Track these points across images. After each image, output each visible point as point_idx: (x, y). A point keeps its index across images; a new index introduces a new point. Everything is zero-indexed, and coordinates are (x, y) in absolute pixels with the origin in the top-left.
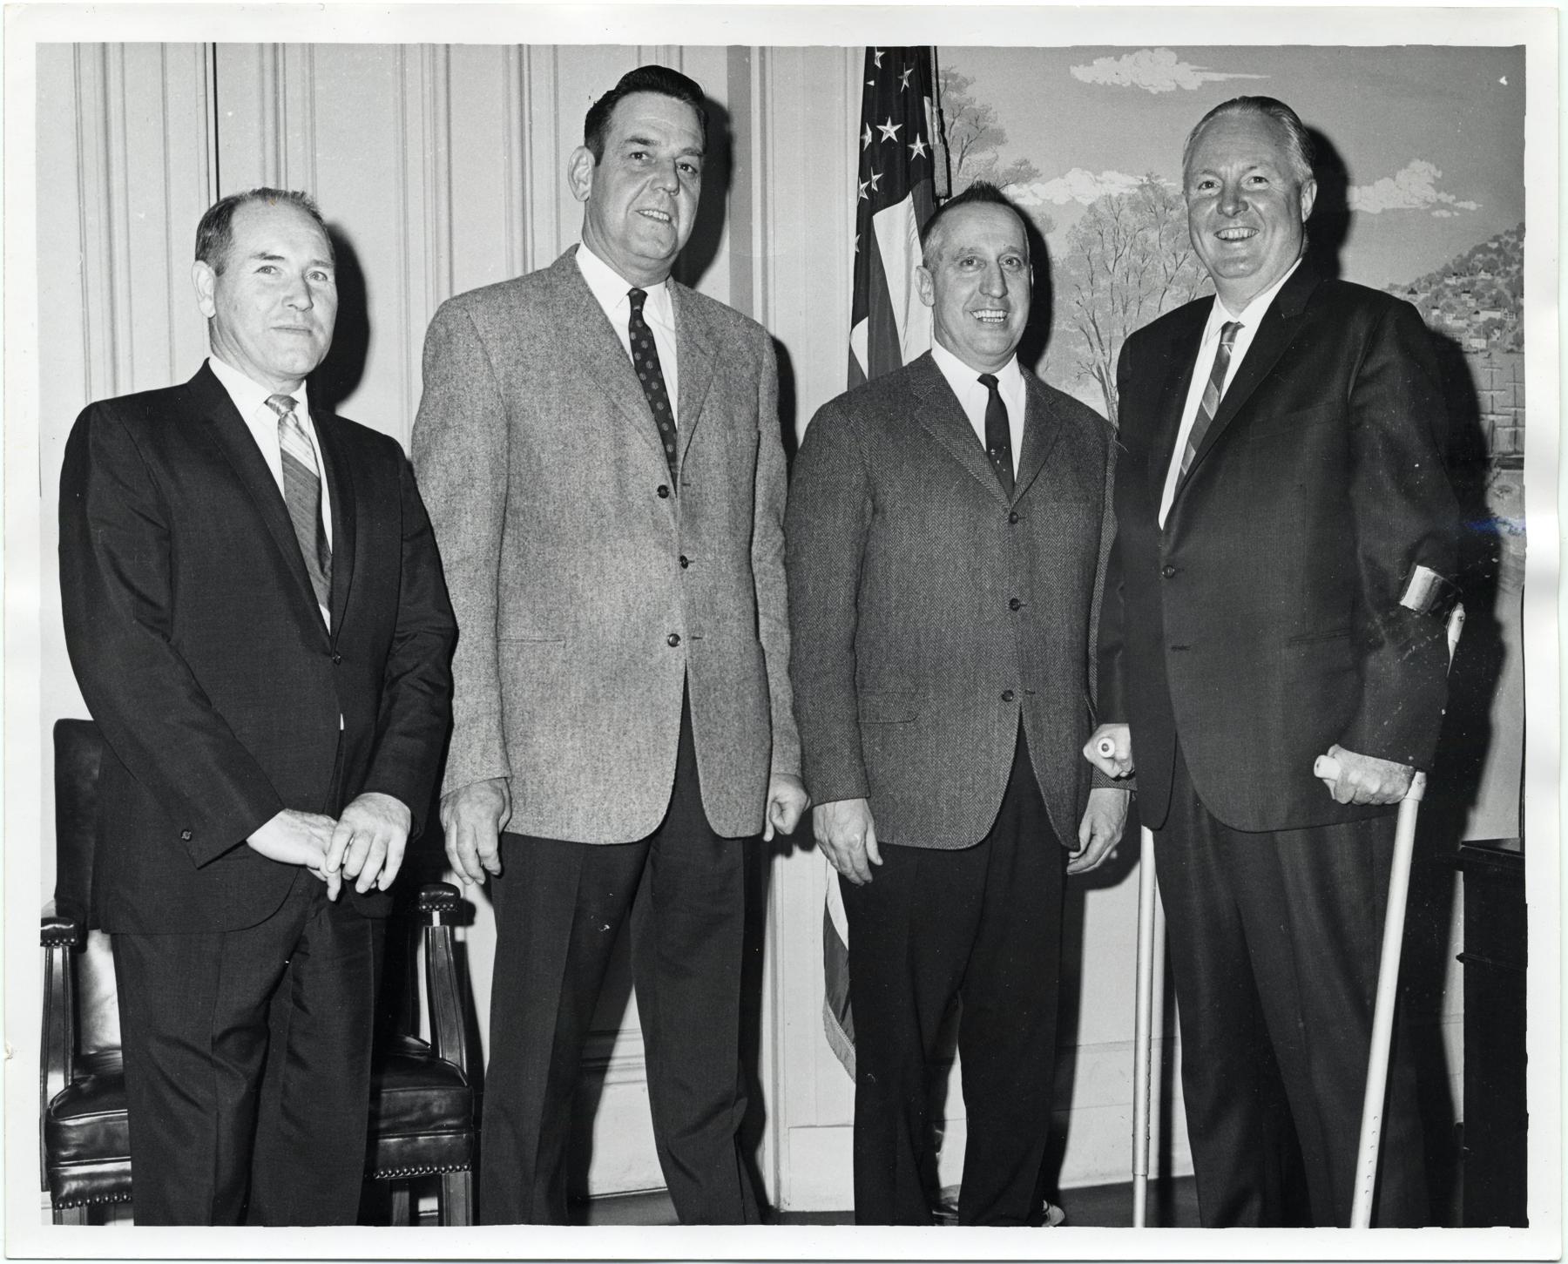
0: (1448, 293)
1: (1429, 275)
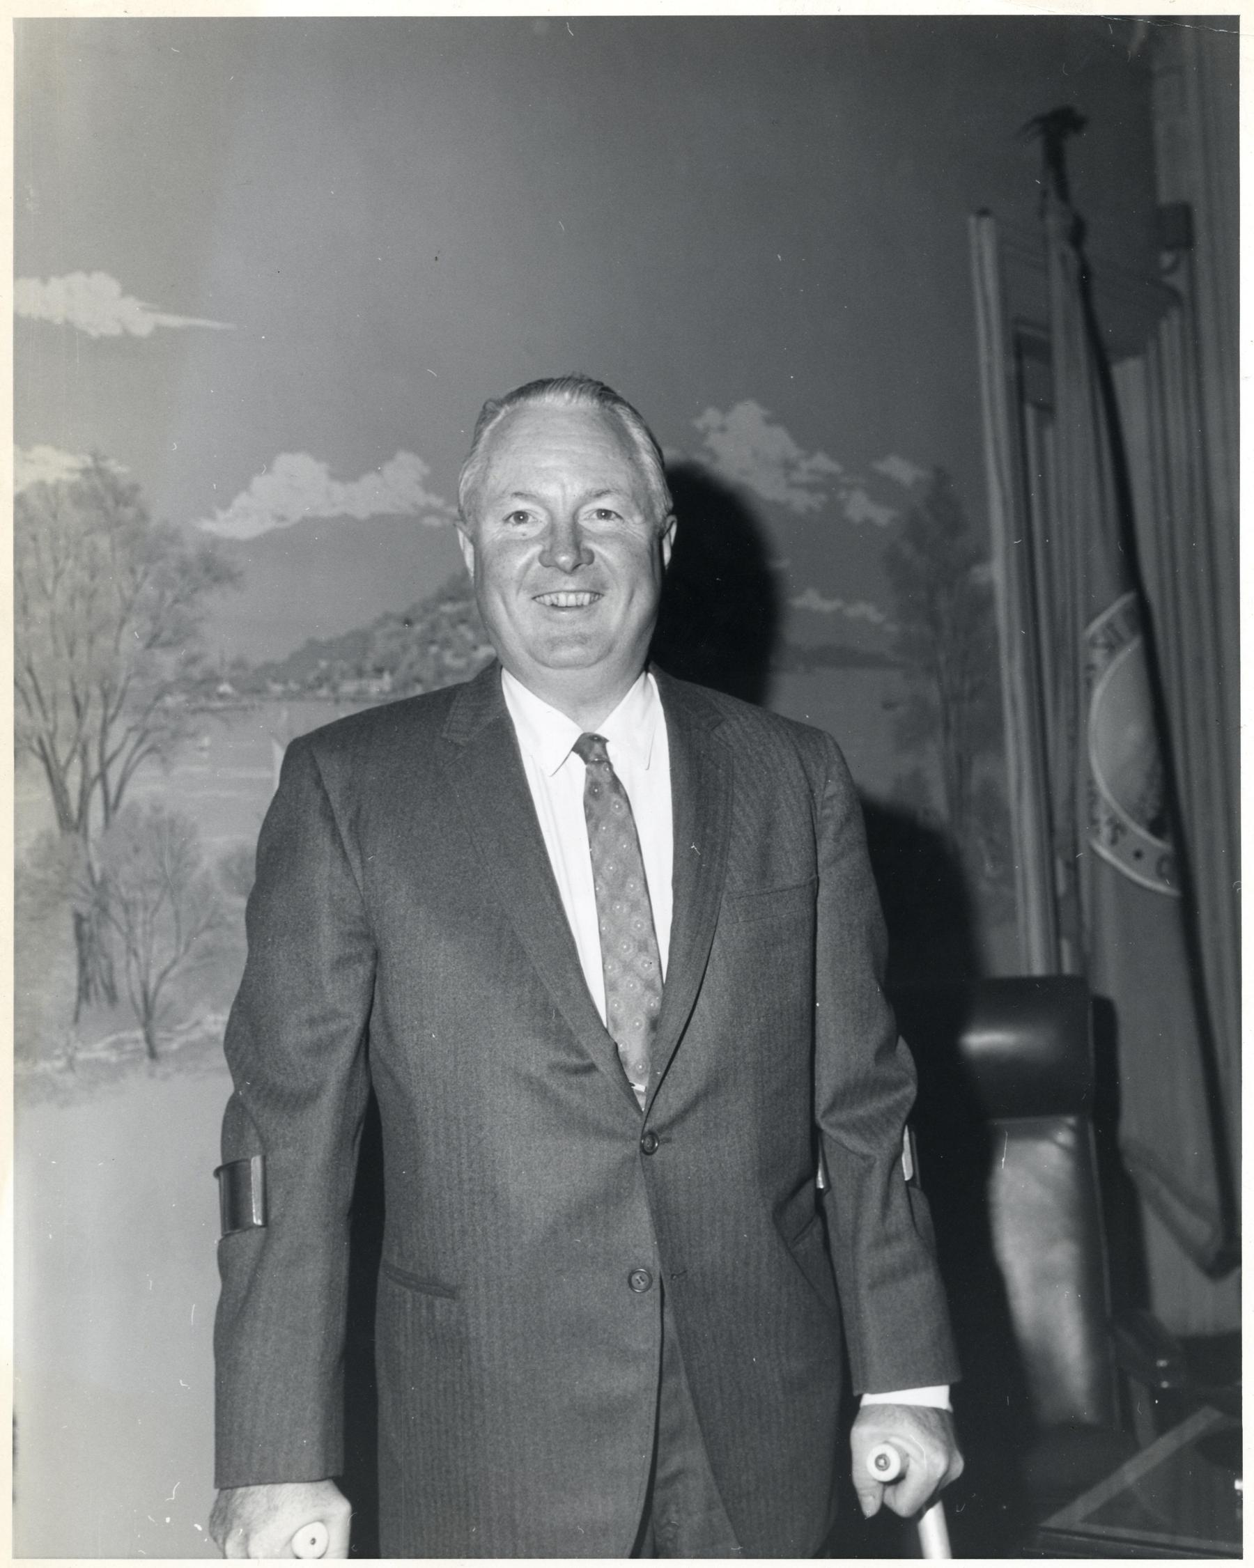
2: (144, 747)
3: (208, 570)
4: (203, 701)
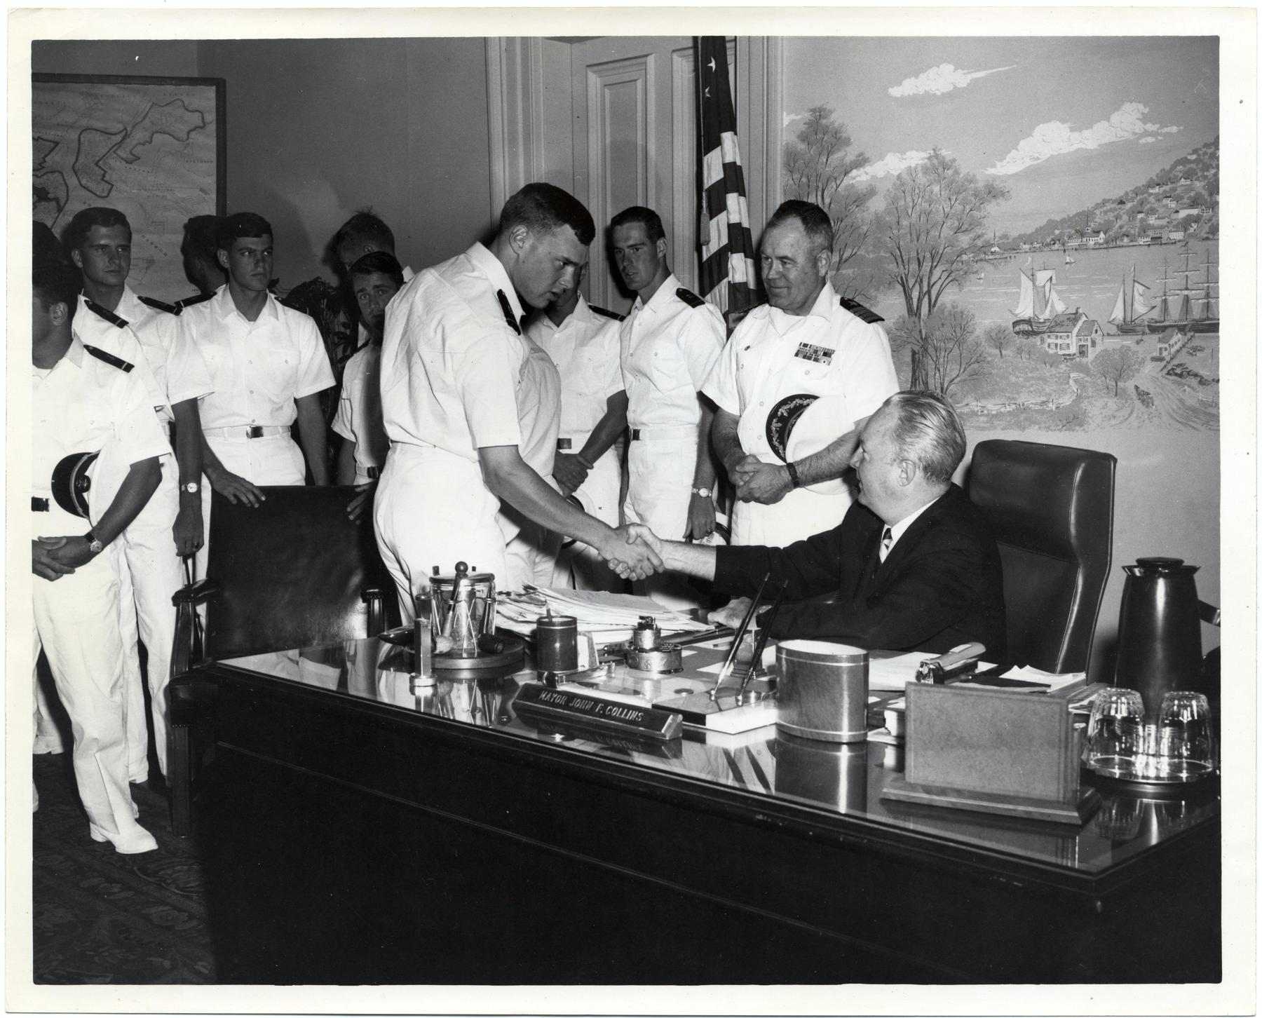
0: (1152, 199)
1: (1136, 188)
2: (950, 279)
3: (990, 193)
4: (983, 256)
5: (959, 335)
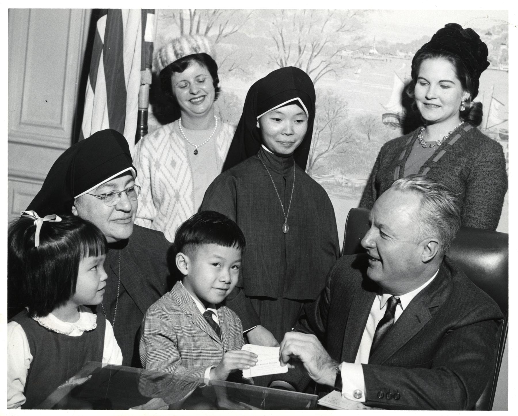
2: (328, 69)
4: (361, 55)
5: (331, 117)
